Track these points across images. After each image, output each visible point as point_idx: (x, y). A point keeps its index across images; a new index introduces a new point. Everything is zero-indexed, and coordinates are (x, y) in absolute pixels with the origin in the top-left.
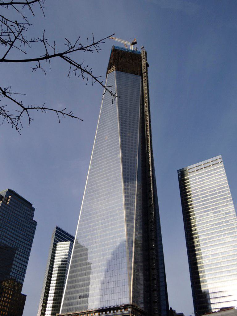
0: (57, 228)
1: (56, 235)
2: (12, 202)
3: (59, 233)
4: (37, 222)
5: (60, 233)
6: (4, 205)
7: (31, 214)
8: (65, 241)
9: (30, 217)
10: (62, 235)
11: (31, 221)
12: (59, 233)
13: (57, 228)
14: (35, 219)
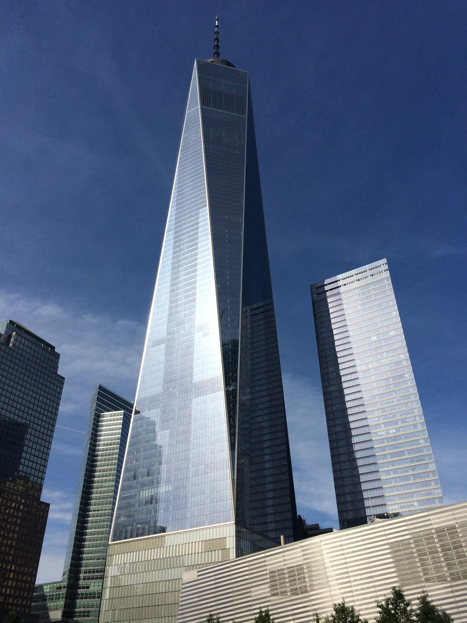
0: (101, 388)
1: (98, 399)
2: (18, 344)
3: (104, 396)
4: (64, 379)
8: (116, 410)
9: (52, 369)
10: (111, 400)
11: (54, 376)
12: (104, 396)
13: (101, 388)
14: (60, 372)
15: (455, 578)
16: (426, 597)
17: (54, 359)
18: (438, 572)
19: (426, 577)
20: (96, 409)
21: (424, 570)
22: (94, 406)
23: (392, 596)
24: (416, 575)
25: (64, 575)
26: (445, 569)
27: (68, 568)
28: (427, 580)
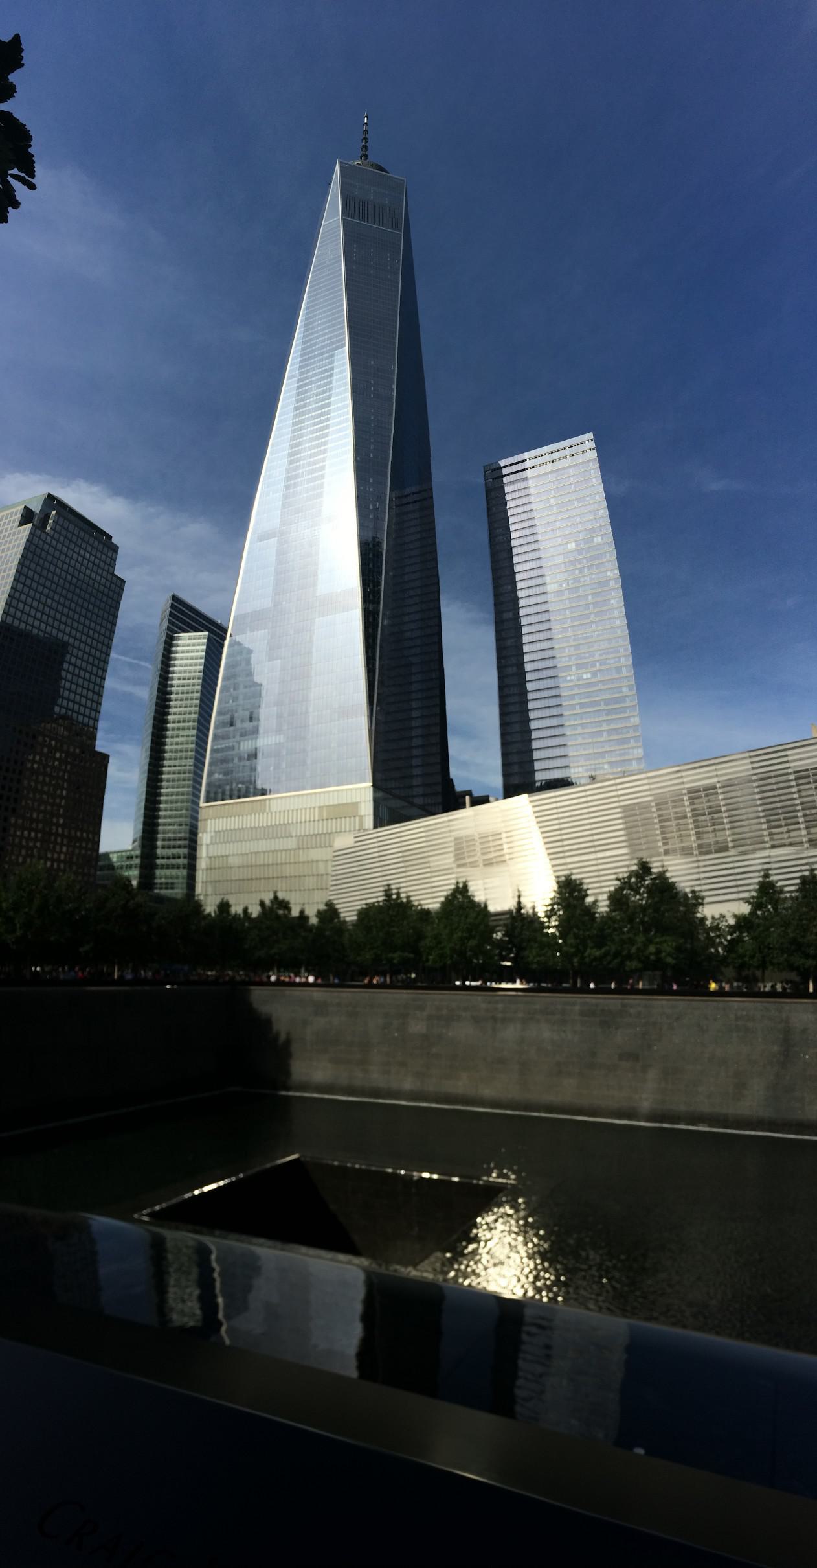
0: (175, 598)
1: (171, 614)
2: (58, 528)
3: (180, 611)
5: (183, 613)
6: (38, 532)
7: (108, 560)
10: (190, 617)
12: (180, 611)
15: (704, 850)
16: (664, 872)
17: (110, 554)
18: (682, 841)
19: (666, 847)
20: (168, 628)
21: (663, 839)
22: (166, 624)
23: (635, 868)
24: (653, 845)
25: (134, 841)
26: (693, 838)
27: (140, 834)
28: (666, 852)
